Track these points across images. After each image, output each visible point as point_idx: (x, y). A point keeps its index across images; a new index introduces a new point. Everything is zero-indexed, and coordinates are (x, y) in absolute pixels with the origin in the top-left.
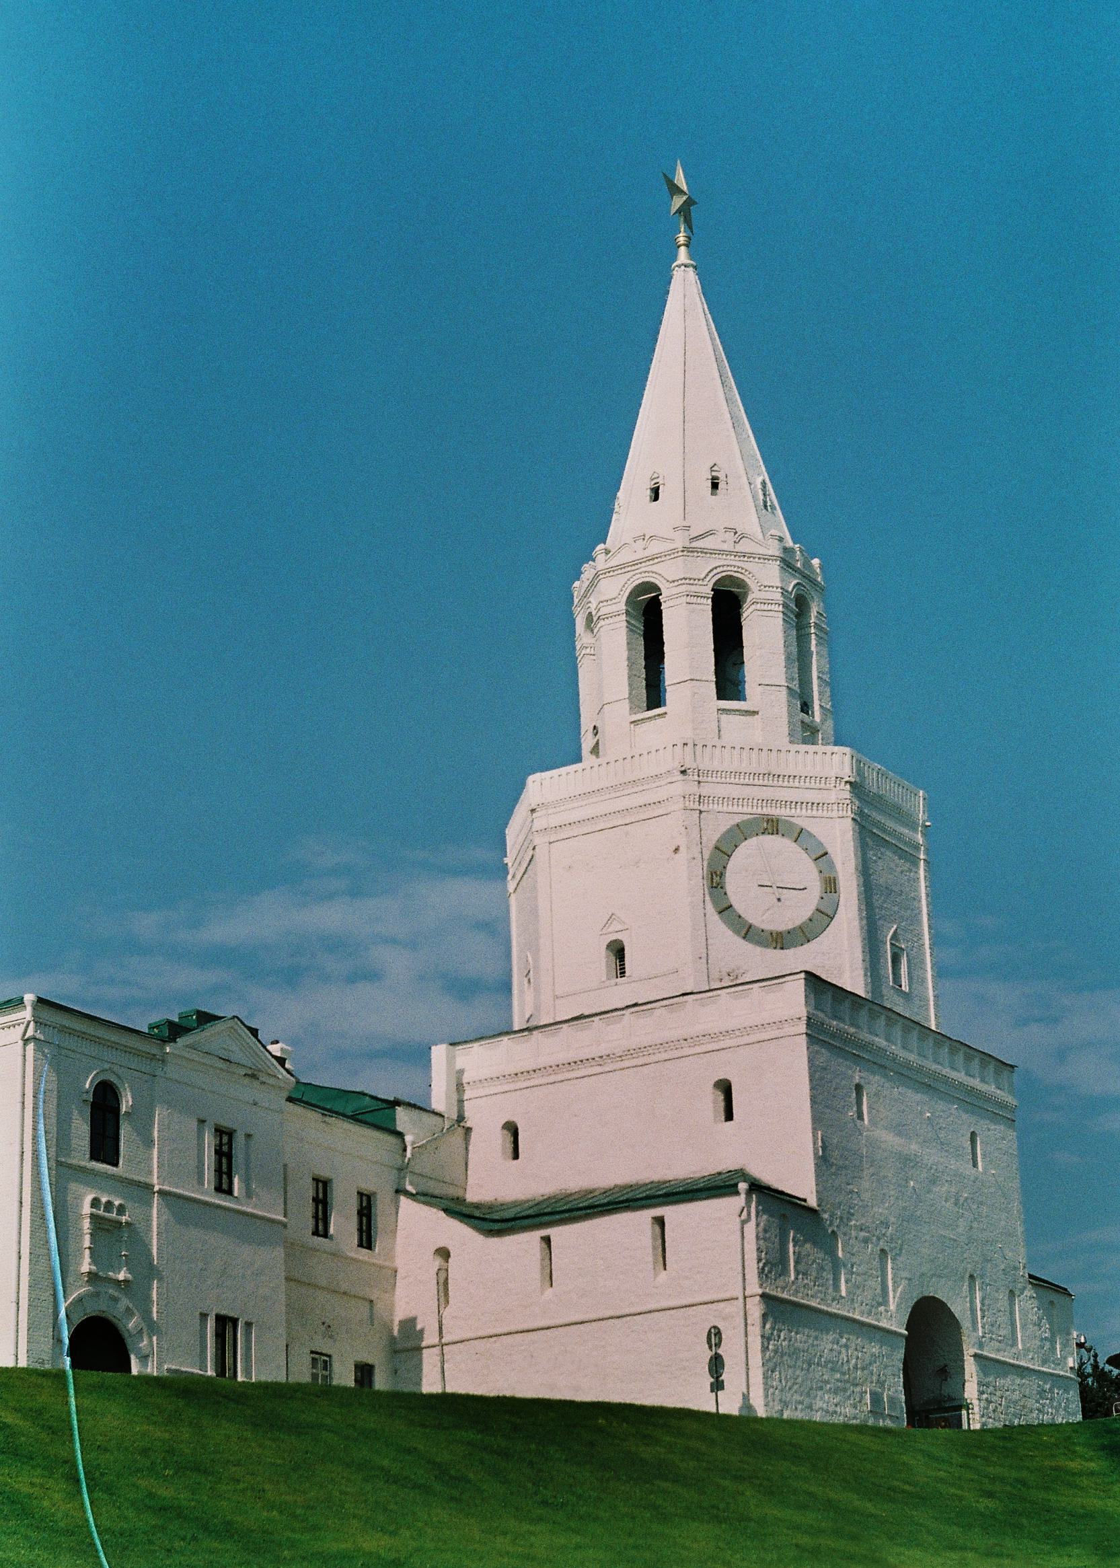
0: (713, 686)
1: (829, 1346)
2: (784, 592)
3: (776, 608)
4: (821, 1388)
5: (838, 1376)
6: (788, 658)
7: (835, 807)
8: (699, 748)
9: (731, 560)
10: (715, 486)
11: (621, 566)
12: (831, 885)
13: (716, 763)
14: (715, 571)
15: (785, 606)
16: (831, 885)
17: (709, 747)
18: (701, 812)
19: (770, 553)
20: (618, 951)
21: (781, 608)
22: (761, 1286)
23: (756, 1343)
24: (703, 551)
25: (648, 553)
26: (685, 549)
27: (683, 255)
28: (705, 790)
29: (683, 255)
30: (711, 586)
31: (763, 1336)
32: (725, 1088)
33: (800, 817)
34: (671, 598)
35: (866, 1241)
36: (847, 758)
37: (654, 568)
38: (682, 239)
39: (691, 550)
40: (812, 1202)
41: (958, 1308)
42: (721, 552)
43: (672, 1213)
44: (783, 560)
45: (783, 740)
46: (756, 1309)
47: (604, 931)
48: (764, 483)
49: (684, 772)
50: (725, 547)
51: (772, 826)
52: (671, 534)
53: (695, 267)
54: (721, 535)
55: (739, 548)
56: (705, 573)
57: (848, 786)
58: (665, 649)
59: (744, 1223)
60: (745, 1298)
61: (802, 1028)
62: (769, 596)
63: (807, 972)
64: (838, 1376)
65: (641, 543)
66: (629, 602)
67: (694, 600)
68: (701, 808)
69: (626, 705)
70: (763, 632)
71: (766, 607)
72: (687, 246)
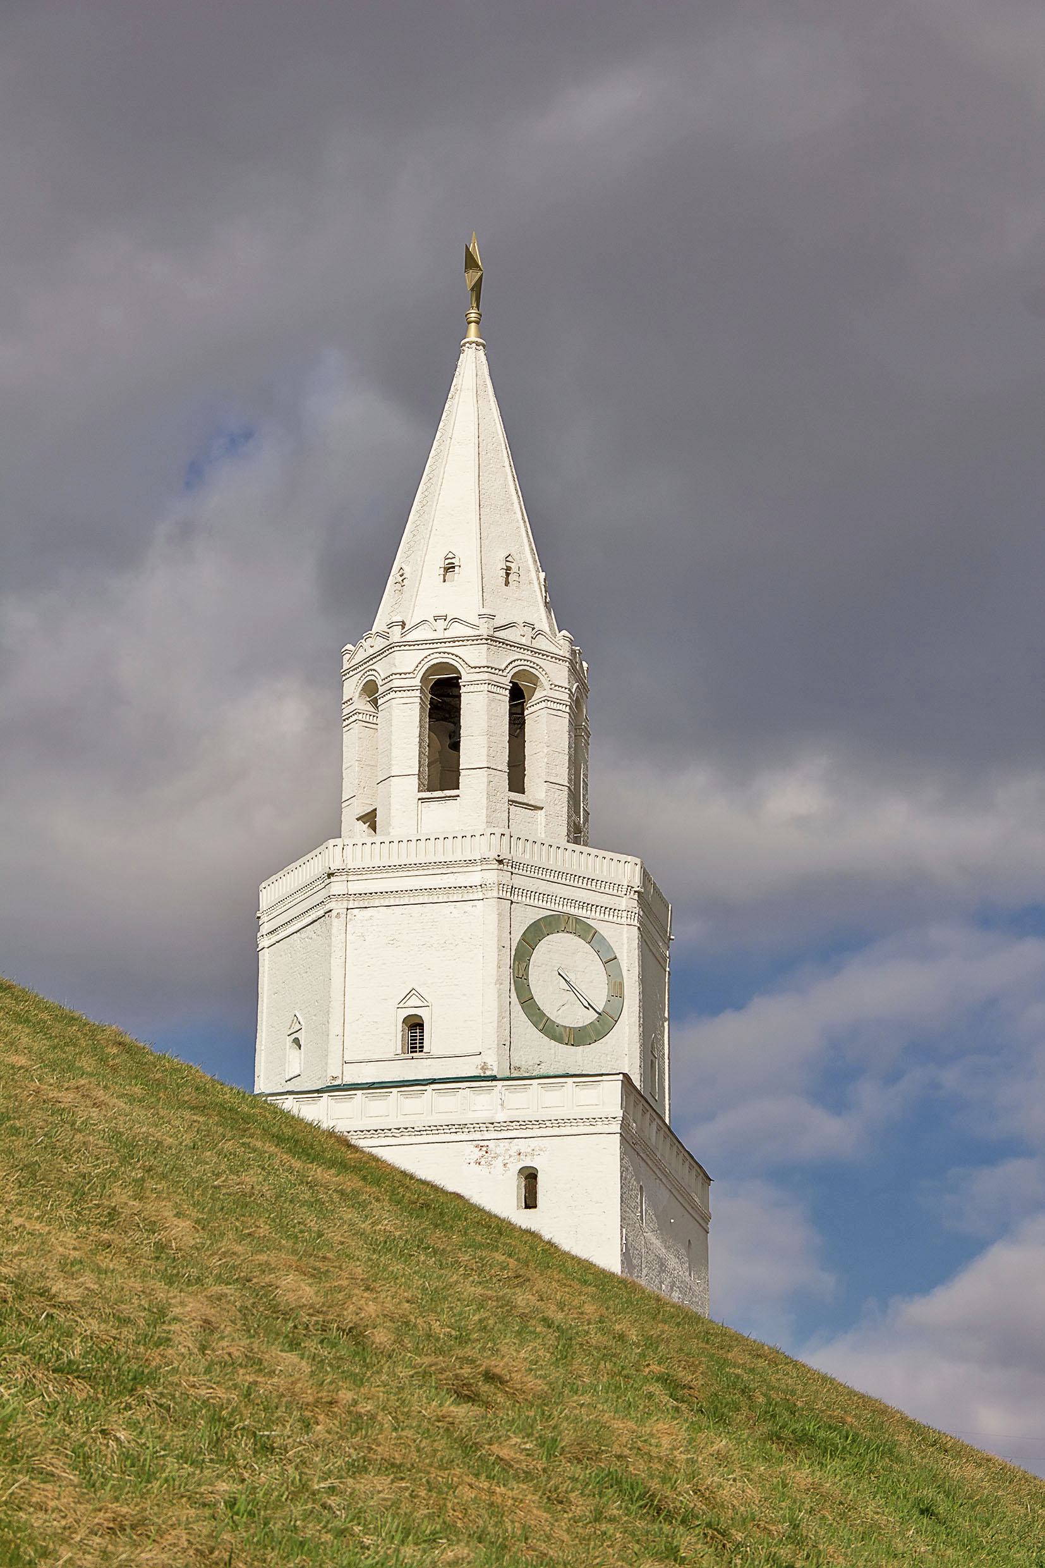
3: (563, 708)
7: (625, 914)
9: (527, 655)
11: (416, 643)
12: (617, 990)
13: (527, 856)
14: (514, 664)
16: (617, 990)
17: (538, 843)
19: (561, 653)
20: (415, 1025)
21: (567, 709)
24: (504, 643)
25: (448, 634)
28: (518, 881)
32: (530, 1177)
33: (594, 919)
34: (471, 683)
38: (473, 316)
39: (491, 639)
45: (563, 841)
47: (401, 1005)
49: (500, 862)
50: (523, 641)
53: (484, 346)
54: (521, 630)
57: (636, 897)
61: (616, 1127)
62: (557, 695)
63: (625, 1075)
65: (441, 624)
66: (424, 679)
67: (494, 689)
68: (515, 899)
69: (415, 781)
70: (548, 730)
72: (477, 323)
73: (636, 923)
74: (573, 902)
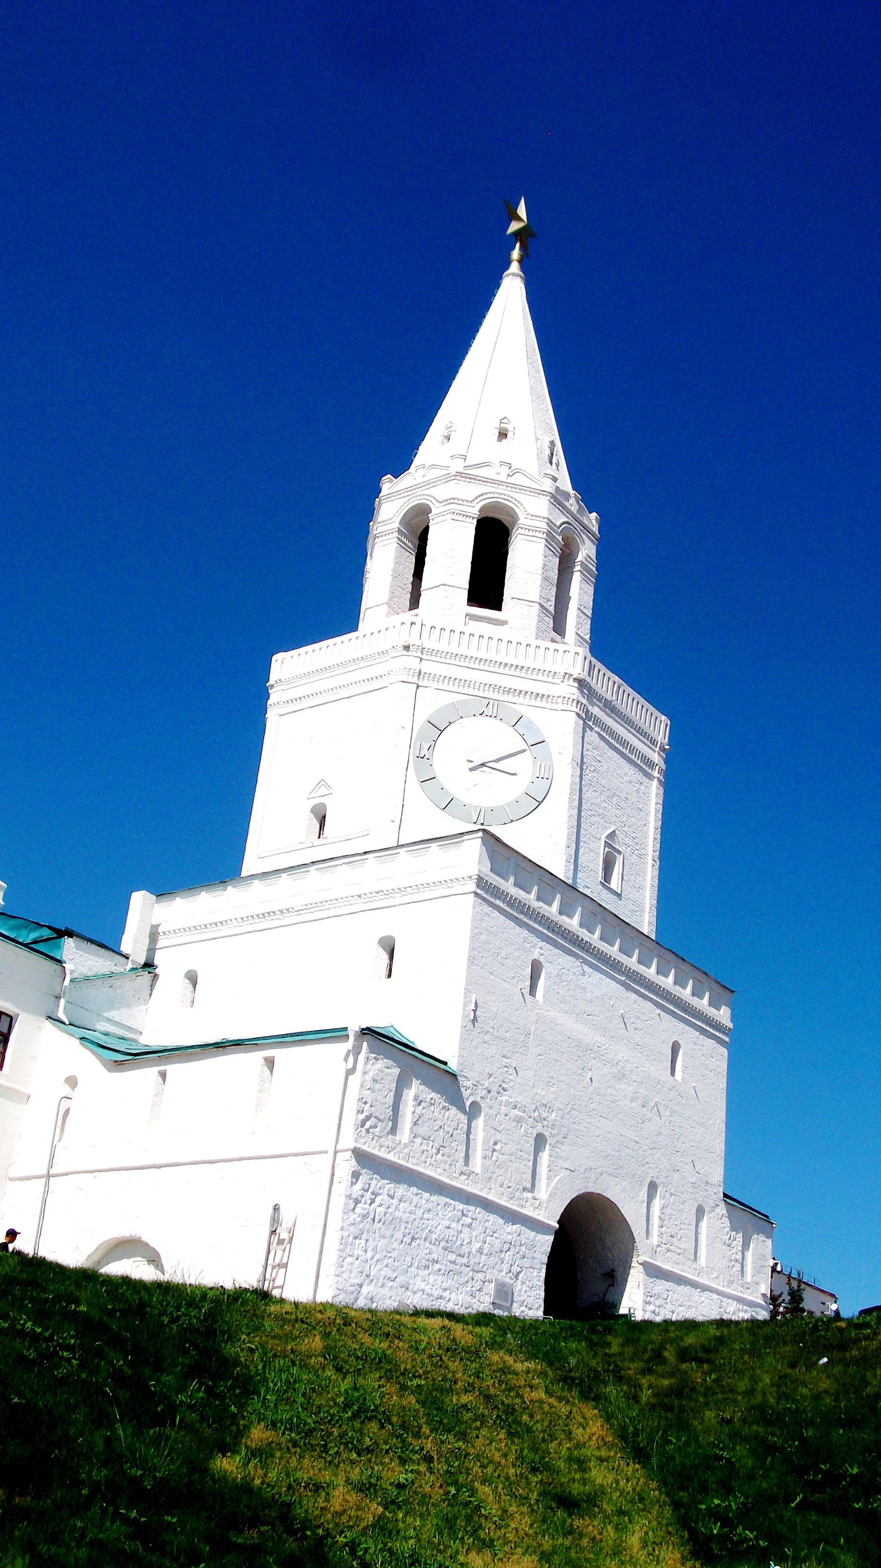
0: (466, 592)
1: (447, 1223)
2: (550, 523)
3: (541, 535)
4: (427, 1267)
5: (453, 1257)
6: (546, 579)
7: (560, 700)
8: (426, 630)
9: (501, 489)
10: (503, 435)
14: (485, 496)
15: (549, 534)
18: (418, 686)
21: (545, 536)
22: (356, 1141)
23: (338, 1202)
26: (459, 473)
27: (515, 267)
28: (426, 667)
29: (515, 267)
30: (478, 507)
31: (349, 1197)
34: (438, 515)
35: (519, 1120)
36: (580, 658)
37: (429, 492)
40: (453, 1066)
41: (631, 1210)
42: (494, 482)
43: (280, 1054)
44: (553, 496)
46: (346, 1165)
48: (552, 443)
51: (488, 709)
52: (447, 461)
54: (497, 469)
55: (510, 480)
56: (473, 499)
57: (576, 685)
58: (427, 559)
59: (351, 1072)
60: (336, 1153)
61: (472, 886)
64: (453, 1257)
67: (457, 517)
71: (530, 533)
73: (574, 708)
74: (497, 688)
